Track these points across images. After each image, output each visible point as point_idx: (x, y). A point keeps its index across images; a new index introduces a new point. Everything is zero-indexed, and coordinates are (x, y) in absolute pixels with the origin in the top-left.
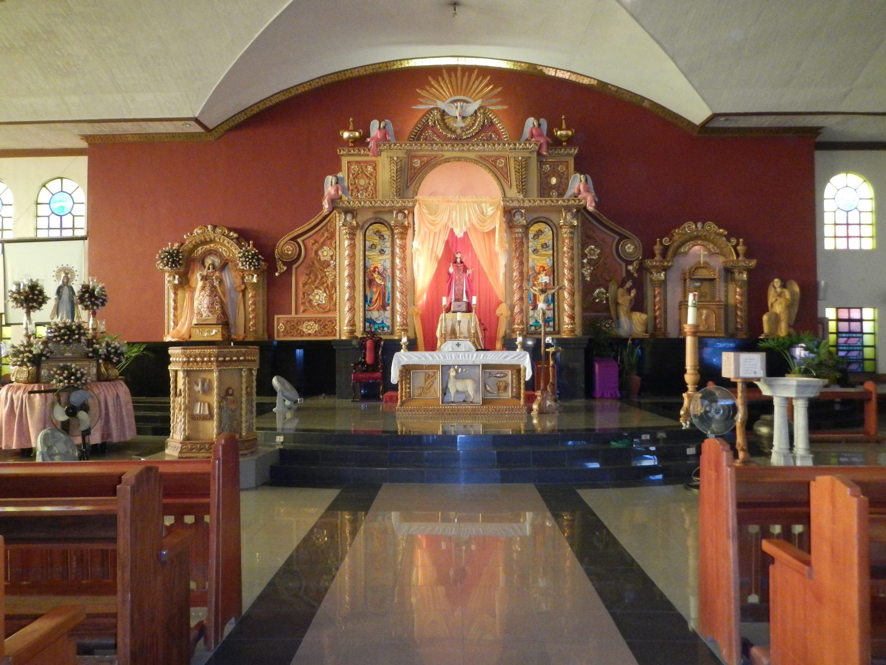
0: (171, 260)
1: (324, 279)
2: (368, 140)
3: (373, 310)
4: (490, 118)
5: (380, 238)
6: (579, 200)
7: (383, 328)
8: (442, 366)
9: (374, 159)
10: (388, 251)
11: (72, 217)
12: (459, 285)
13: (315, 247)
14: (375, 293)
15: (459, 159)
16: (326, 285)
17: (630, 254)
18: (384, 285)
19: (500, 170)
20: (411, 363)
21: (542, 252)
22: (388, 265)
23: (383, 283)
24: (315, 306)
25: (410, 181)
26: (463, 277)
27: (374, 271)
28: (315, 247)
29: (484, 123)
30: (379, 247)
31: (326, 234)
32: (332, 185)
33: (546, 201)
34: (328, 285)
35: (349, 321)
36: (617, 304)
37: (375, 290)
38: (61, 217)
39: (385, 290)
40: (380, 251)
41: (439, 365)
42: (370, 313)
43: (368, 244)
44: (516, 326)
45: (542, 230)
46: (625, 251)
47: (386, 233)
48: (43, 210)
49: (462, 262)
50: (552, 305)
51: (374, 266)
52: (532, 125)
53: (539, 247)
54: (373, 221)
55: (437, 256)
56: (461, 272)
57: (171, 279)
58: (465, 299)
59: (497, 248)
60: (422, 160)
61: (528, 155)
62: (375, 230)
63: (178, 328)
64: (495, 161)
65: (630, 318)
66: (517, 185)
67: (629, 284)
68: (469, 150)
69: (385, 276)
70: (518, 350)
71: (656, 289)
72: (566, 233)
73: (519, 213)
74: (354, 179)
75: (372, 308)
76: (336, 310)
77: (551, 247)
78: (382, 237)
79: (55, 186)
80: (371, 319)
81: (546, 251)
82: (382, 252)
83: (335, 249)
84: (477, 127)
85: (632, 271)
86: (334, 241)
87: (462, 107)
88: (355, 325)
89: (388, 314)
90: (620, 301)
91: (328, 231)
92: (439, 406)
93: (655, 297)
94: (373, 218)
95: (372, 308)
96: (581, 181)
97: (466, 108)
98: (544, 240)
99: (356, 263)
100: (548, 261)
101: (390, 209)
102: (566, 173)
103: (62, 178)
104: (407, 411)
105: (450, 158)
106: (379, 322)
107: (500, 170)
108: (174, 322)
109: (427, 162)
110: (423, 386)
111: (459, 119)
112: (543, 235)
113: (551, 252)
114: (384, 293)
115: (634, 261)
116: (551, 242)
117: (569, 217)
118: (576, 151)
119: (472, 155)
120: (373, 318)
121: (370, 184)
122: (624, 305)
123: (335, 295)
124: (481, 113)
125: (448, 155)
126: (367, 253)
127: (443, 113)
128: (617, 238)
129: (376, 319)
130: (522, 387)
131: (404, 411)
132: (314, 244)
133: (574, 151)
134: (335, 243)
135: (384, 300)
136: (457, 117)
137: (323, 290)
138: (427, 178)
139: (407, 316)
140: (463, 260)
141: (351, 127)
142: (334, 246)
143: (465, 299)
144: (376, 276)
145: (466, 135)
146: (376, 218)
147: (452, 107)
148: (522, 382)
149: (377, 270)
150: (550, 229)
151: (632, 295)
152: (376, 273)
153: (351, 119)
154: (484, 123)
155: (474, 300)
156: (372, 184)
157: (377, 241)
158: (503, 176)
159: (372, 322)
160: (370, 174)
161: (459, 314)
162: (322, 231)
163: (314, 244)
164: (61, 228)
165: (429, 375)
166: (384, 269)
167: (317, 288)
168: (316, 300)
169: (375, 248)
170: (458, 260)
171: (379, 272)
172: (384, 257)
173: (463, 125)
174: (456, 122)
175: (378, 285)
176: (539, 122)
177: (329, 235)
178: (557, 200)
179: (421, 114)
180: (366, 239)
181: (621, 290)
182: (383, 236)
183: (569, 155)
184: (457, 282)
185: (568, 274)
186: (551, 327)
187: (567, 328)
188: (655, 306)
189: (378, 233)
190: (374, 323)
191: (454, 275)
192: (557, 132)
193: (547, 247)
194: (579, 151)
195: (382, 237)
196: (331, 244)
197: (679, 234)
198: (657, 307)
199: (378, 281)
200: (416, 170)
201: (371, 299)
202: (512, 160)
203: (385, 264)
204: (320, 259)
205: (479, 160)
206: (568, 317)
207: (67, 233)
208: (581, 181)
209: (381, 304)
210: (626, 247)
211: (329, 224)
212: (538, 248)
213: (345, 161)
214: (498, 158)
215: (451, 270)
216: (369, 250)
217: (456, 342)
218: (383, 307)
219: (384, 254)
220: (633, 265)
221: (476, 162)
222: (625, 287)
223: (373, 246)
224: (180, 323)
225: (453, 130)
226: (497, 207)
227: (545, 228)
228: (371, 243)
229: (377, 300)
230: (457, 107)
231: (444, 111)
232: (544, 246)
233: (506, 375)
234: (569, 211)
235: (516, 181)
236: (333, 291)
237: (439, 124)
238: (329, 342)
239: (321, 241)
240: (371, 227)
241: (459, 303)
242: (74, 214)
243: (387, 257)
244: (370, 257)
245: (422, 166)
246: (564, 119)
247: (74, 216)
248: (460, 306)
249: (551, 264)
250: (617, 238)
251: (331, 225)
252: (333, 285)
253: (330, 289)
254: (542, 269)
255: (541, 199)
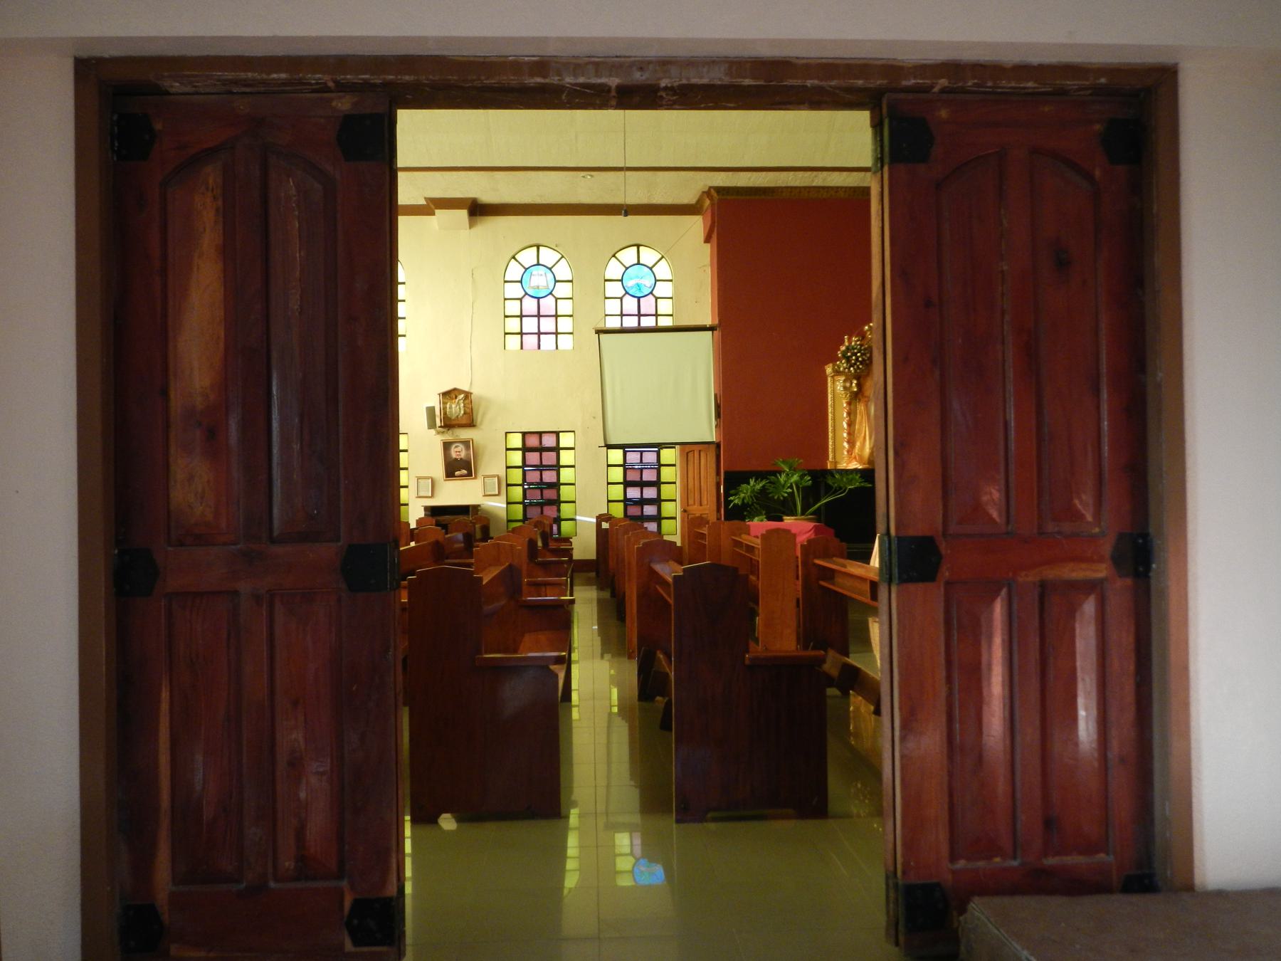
0: (860, 359)
11: (520, 297)
38: (639, 298)
48: (614, 289)
57: (848, 385)
63: (856, 450)
79: (629, 256)
103: (638, 246)
108: (848, 442)
164: (639, 315)
207: (648, 322)
224: (858, 444)
242: (657, 296)
247: (657, 299)
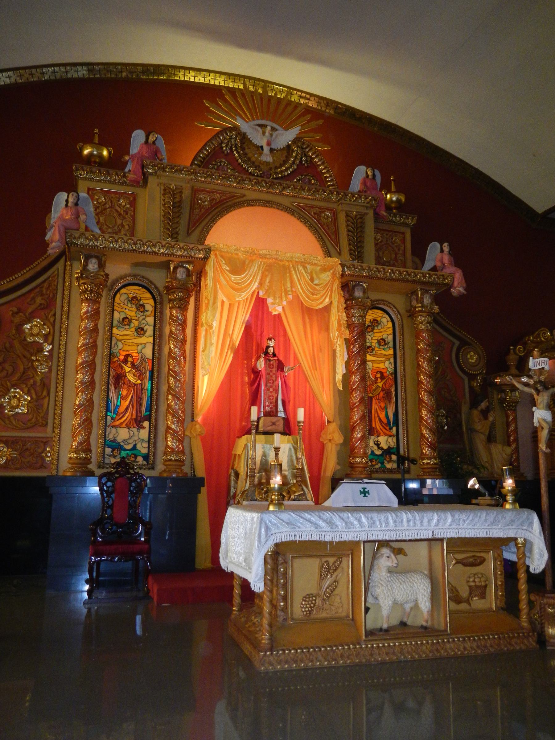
1: (29, 373)
2: (127, 158)
3: (120, 426)
4: (311, 157)
5: (138, 309)
6: (443, 276)
7: (136, 456)
8: (364, 542)
9: (131, 191)
10: (150, 330)
12: (271, 390)
13: (17, 320)
14: (124, 398)
15: (267, 204)
16: (32, 381)
17: (473, 366)
18: (141, 384)
19: (326, 228)
20: (298, 538)
21: (380, 351)
22: (148, 352)
23: (139, 382)
24: (9, 417)
25: (192, 227)
26: (277, 378)
27: (125, 361)
28: (17, 320)
29: (301, 161)
30: (135, 323)
31: (39, 300)
32: (67, 205)
33: (400, 273)
34: (35, 383)
35: (80, 444)
36: (471, 430)
37: (124, 392)
39: (142, 394)
40: (136, 330)
41: (359, 542)
42: (114, 430)
43: (116, 315)
44: (358, 460)
45: (379, 319)
46: (467, 359)
47: (149, 305)
49: (274, 355)
50: (394, 429)
51: (124, 353)
52: (365, 175)
53: (374, 344)
54: (130, 280)
55: (233, 344)
56: (274, 370)
58: (282, 414)
59: (334, 334)
60: (215, 197)
61: (363, 210)
62: (131, 296)
64: (319, 215)
65: (490, 454)
66: (350, 250)
67: (484, 405)
68: (281, 194)
69: (143, 371)
70: (508, 506)
71: (509, 413)
72: (421, 323)
73: (361, 287)
74: (97, 214)
75: (117, 423)
76: (46, 425)
77: (391, 344)
78: (141, 307)
80: (114, 441)
81: (383, 349)
82: (140, 331)
83: (53, 325)
84: (291, 167)
85: (477, 389)
86: (52, 313)
87: (271, 135)
88: (90, 451)
89: (144, 434)
90: (478, 426)
91: (42, 295)
92: (359, 644)
93: (508, 425)
94: (130, 275)
95: (117, 423)
96: (442, 251)
97: (276, 137)
98: (381, 334)
99: (98, 343)
100: (387, 363)
101: (164, 259)
102: (402, 248)
104: (287, 662)
105: (253, 201)
106: (129, 447)
107: (326, 228)
109: (220, 202)
110: (314, 592)
111: (266, 149)
112: (379, 327)
113: (391, 352)
114: (141, 399)
115: (477, 375)
116: (390, 338)
117: (427, 300)
118: (415, 221)
119: (286, 201)
120: (119, 439)
121: (123, 226)
122: (482, 433)
123: (46, 401)
124: (298, 147)
125: (251, 195)
126: (115, 331)
127: (244, 137)
128: (457, 343)
129: (124, 441)
130: (523, 586)
131: (279, 663)
132: (14, 314)
133: (412, 221)
134: (55, 315)
135: (139, 411)
136: (262, 147)
137: (26, 390)
138: (213, 230)
139: (183, 438)
140: (276, 353)
141: (96, 140)
142: (52, 320)
143: (282, 414)
144: (127, 369)
145: (276, 173)
146: (135, 276)
147: (257, 131)
148: (522, 576)
149: (130, 359)
150: (389, 319)
151: (491, 419)
152: (129, 364)
153: (96, 131)
154: (301, 161)
155: (301, 414)
156: (127, 227)
157: (133, 314)
158: (330, 236)
159: (116, 447)
160: (124, 211)
161: (276, 434)
162: (32, 295)
163: (17, 313)
165: (329, 569)
166: (143, 360)
167: (14, 386)
168: (13, 408)
169: (129, 325)
170: (271, 350)
171: (133, 363)
172: (143, 340)
173: (269, 159)
174: (261, 154)
175: (131, 385)
176: (374, 171)
177: (43, 302)
178: (414, 273)
179: (215, 133)
180: (115, 308)
181: (475, 413)
182: (143, 306)
183: (406, 225)
184: (269, 385)
185: (428, 382)
186: (394, 462)
187: (428, 464)
188: (509, 437)
189: (134, 300)
190: (120, 448)
191: (264, 374)
192: (386, 195)
193: (385, 344)
194: (417, 220)
195: (141, 307)
196: (47, 317)
197: (532, 342)
198: (512, 438)
199: (131, 378)
200: (203, 210)
201: (118, 407)
202: (342, 218)
203: (143, 351)
204: (25, 340)
205: (297, 210)
206: (429, 447)
208: (442, 251)
209: (134, 417)
210: (469, 356)
211: (46, 285)
212: (374, 344)
213: (82, 186)
214: (323, 210)
215: (261, 365)
216: (117, 327)
217: (359, 487)
218: (138, 423)
219: (143, 335)
220: (477, 380)
221: (291, 211)
222: (479, 408)
223: (126, 321)
225: (257, 164)
226: (334, 275)
227: (382, 317)
228: (123, 316)
229: (127, 409)
230: (264, 133)
231: (245, 134)
232: (382, 342)
233: (482, 561)
234: (427, 291)
235: (350, 244)
236: (45, 393)
237: (238, 152)
238: (43, 479)
239: (30, 310)
240: (123, 290)
241: (274, 419)
243: (147, 339)
244: (119, 338)
245: (212, 207)
246: (393, 180)
248: (274, 424)
249: (391, 369)
250: (457, 343)
251: (50, 285)
252: (45, 385)
253: (39, 389)
254: (379, 375)
255: (395, 269)
